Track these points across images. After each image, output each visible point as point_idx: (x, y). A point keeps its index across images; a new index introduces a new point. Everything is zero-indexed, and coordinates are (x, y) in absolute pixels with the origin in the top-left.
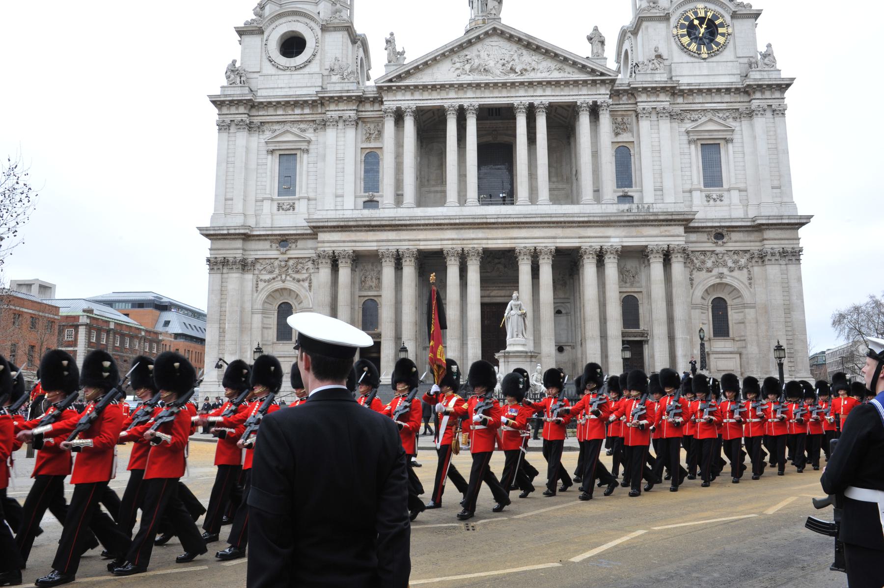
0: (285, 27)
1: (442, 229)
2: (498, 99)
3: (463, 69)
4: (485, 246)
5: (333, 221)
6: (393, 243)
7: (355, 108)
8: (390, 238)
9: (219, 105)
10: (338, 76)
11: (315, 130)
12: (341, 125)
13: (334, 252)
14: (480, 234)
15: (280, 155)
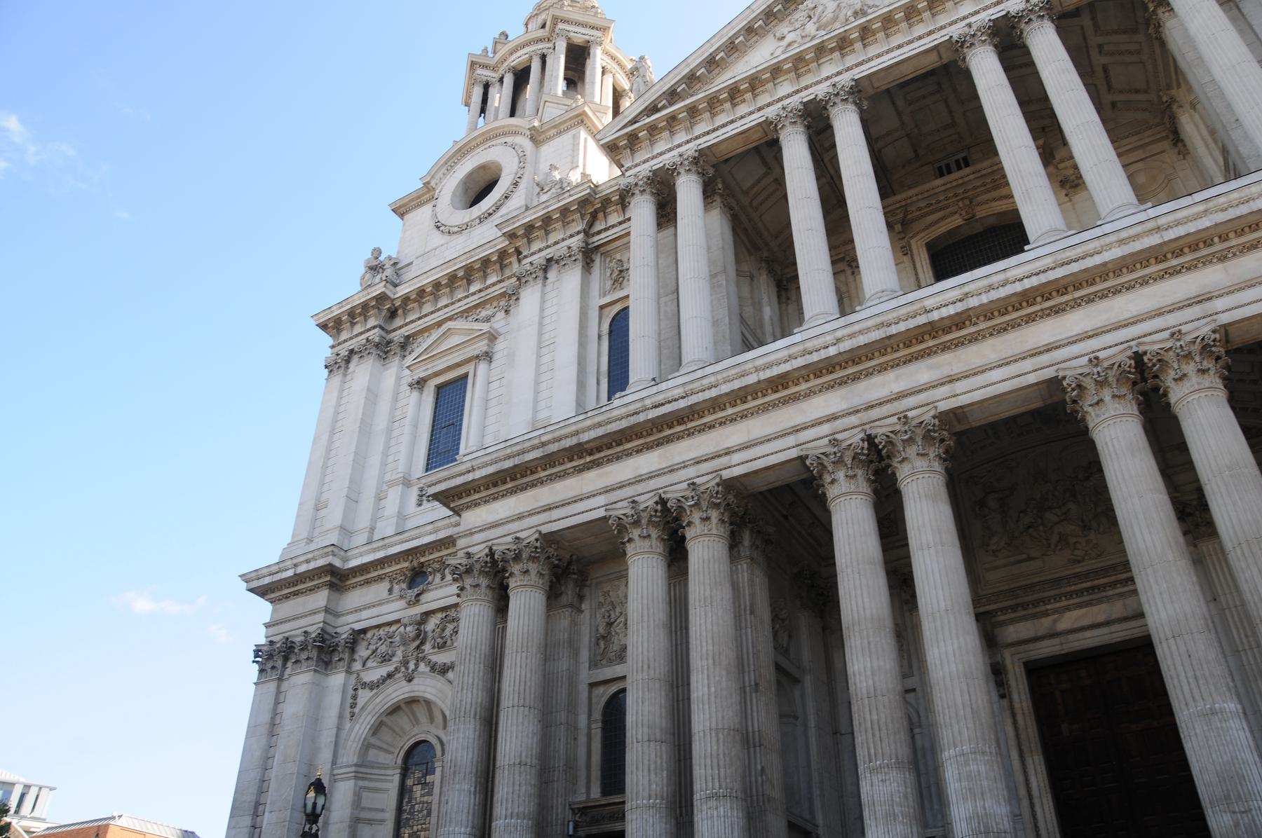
0: (467, 166)
1: (795, 398)
2: (905, 49)
3: (802, 37)
4: (943, 406)
5: (486, 465)
6: (653, 484)
7: (580, 228)
8: (644, 469)
9: (333, 328)
10: (553, 190)
11: (507, 312)
12: (552, 275)
13: (491, 553)
14: (922, 372)
15: (439, 388)
